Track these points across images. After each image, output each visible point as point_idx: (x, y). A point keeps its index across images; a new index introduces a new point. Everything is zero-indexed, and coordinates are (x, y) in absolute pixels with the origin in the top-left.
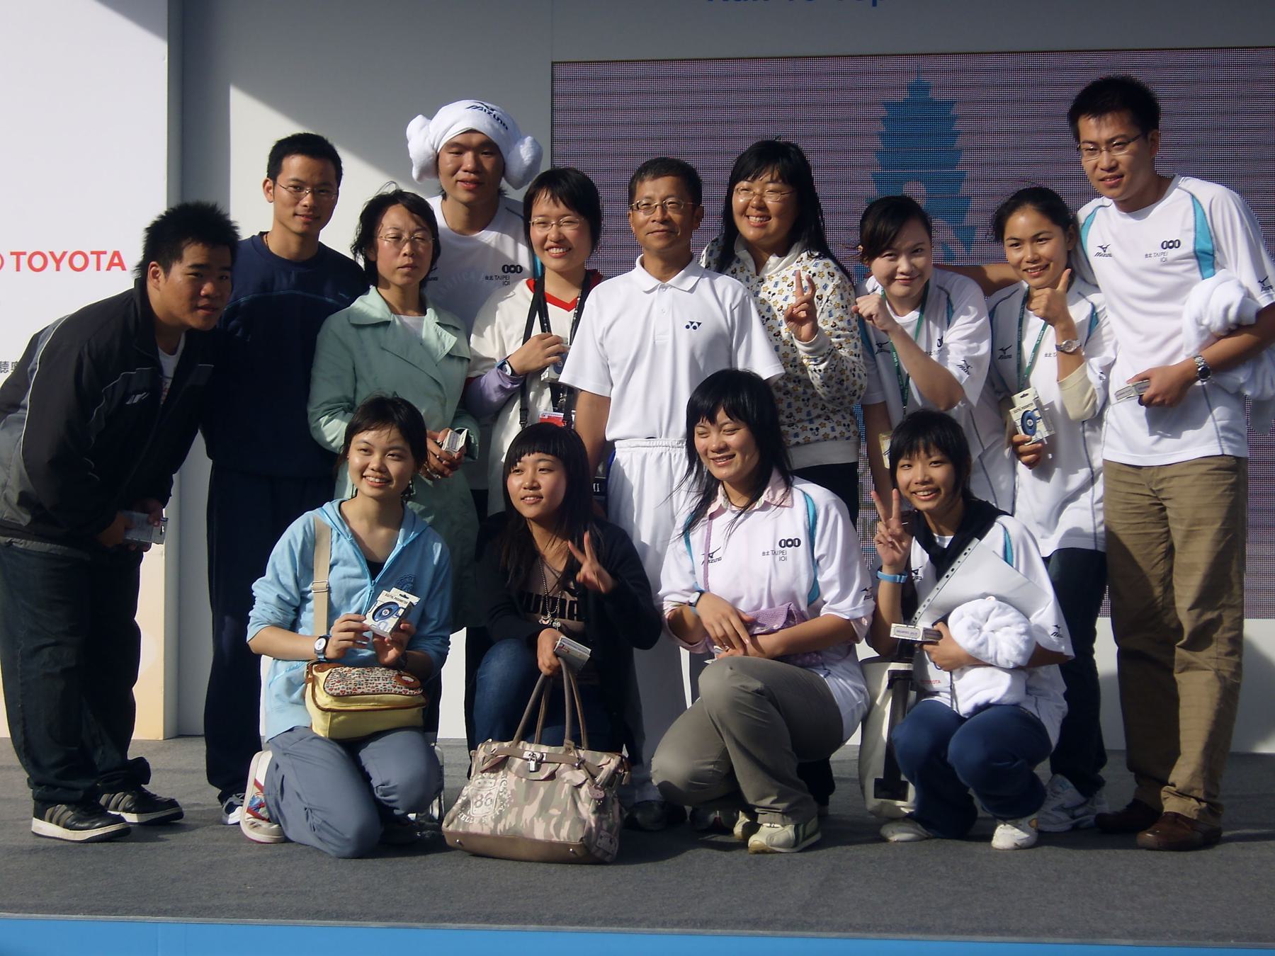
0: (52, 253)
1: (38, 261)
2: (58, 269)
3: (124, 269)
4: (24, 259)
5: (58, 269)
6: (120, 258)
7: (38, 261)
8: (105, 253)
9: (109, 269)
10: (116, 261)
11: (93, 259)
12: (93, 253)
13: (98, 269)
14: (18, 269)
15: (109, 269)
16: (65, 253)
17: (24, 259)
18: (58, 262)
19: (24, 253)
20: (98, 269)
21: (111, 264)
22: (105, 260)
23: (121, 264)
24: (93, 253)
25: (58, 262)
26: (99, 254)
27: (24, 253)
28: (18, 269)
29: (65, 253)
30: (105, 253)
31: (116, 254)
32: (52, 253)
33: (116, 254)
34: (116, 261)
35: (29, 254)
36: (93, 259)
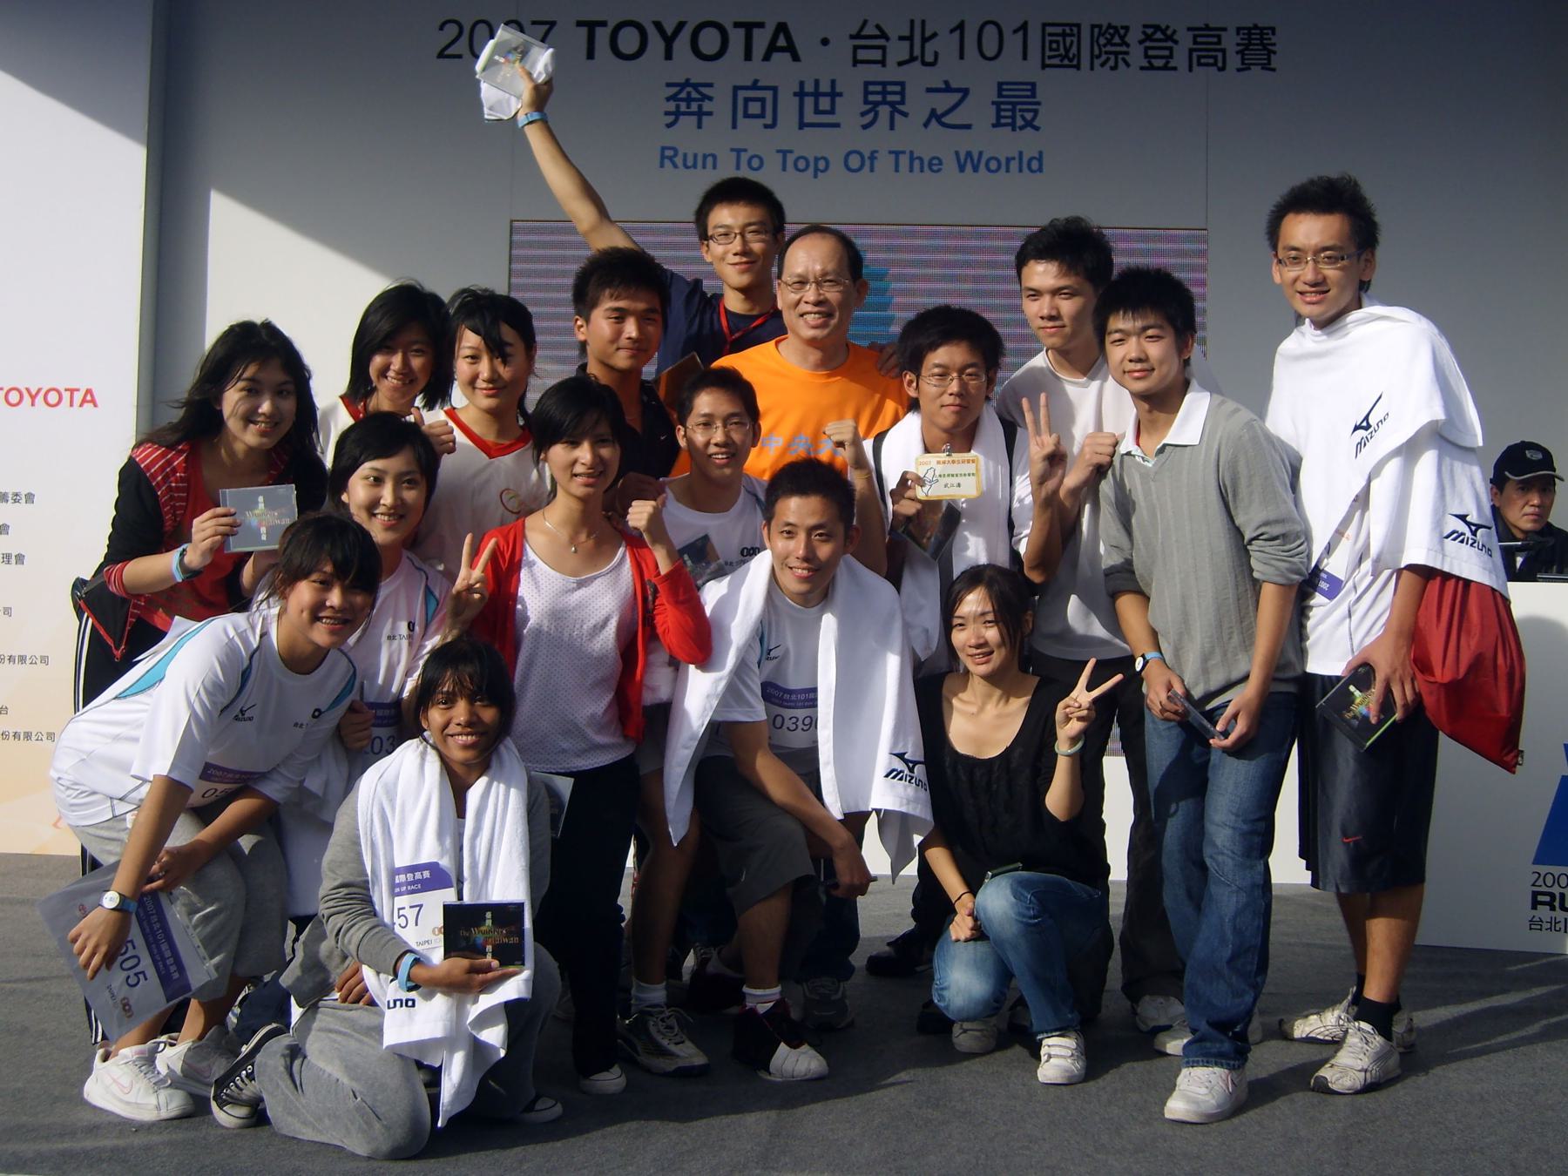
1: (628, 41)
2: (669, 56)
3: (796, 58)
4: (603, 35)
5: (669, 56)
6: (789, 38)
7: (628, 41)
8: (761, 25)
9: (767, 58)
10: (782, 42)
11: (736, 37)
12: (737, 25)
13: (748, 56)
14: (590, 55)
15: (767, 58)
16: (681, 25)
17: (603, 35)
18: (669, 41)
19: (603, 24)
20: (748, 56)
21: (772, 49)
22: (761, 39)
23: (791, 49)
24: (737, 25)
25: (669, 41)
26: (749, 27)
27: (603, 24)
28: (590, 55)
29: (681, 25)
30: (761, 25)
31: (782, 28)
33: (782, 28)
34: (782, 42)
35: (611, 25)
36: (736, 37)
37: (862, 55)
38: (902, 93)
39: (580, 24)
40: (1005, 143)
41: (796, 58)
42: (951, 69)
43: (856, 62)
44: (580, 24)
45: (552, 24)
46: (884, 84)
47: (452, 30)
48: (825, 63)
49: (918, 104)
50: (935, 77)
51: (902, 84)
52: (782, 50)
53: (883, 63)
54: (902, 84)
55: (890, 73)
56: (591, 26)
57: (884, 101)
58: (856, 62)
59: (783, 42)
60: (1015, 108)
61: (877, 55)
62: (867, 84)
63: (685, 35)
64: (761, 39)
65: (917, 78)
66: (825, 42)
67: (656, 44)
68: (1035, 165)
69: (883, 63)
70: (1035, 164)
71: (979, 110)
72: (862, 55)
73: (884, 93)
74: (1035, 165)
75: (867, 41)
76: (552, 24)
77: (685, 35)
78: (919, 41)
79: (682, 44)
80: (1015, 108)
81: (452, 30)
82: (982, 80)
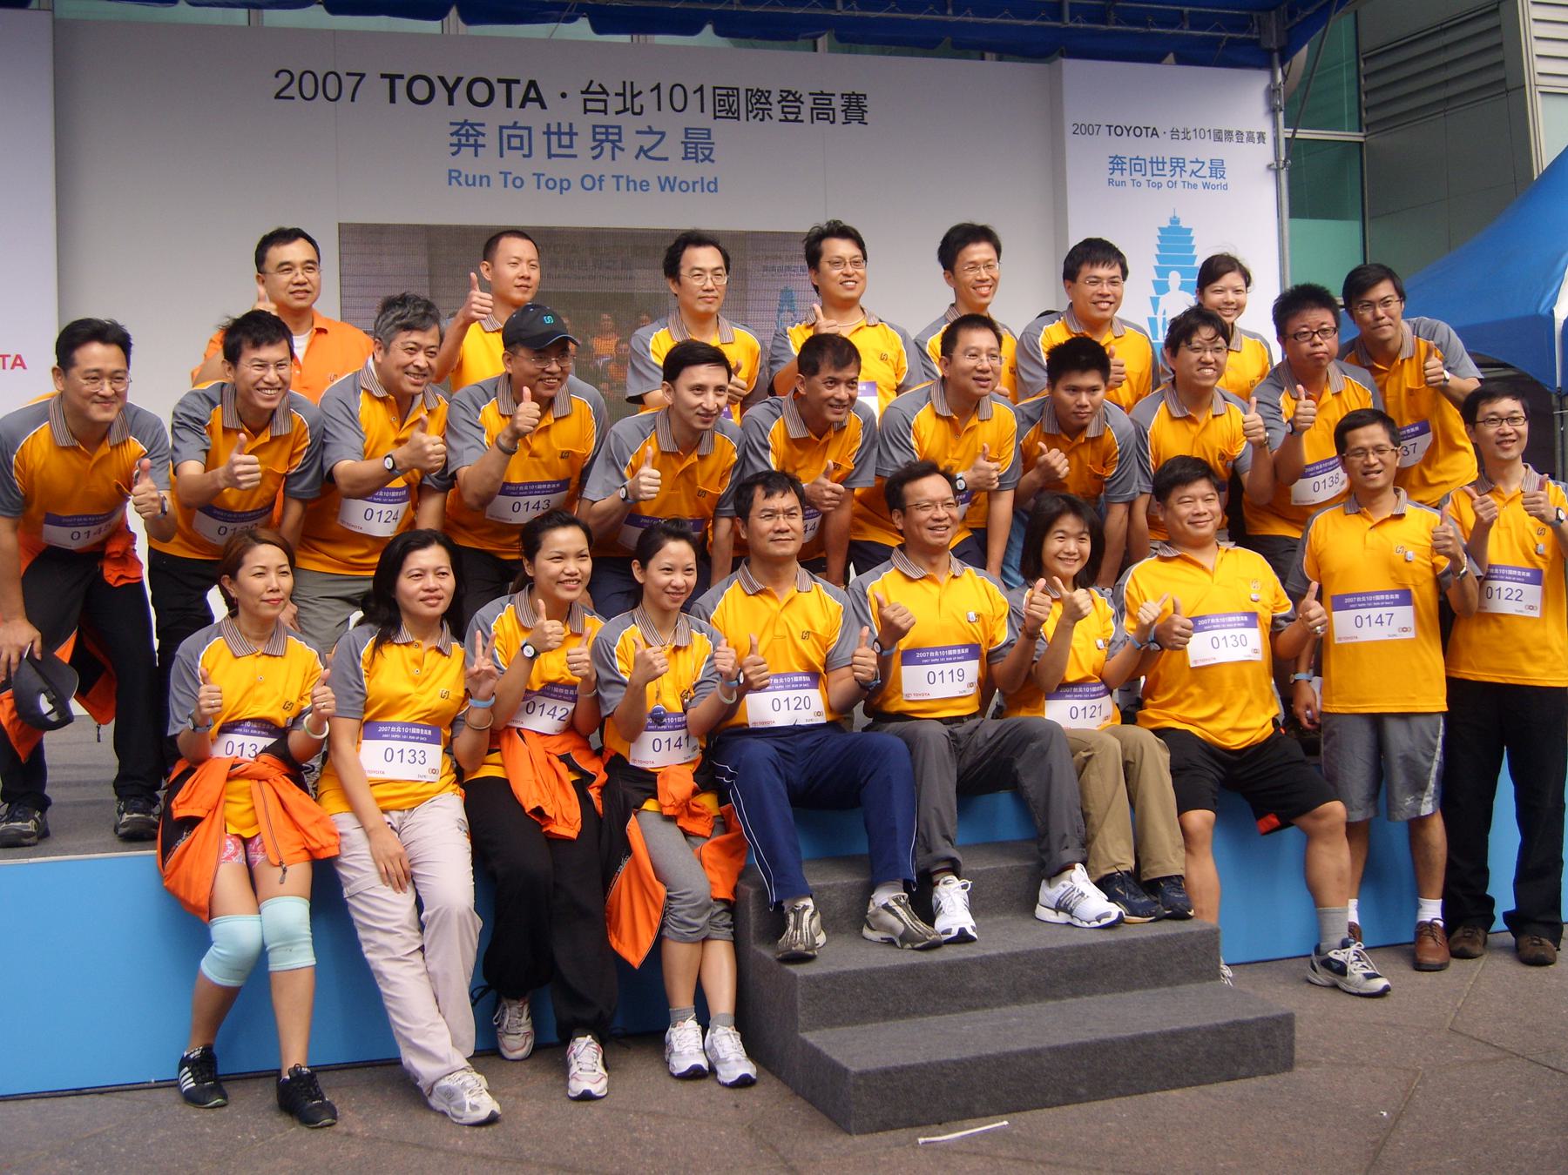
0: (442, 79)
1: (421, 90)
3: (543, 106)
4: (401, 86)
6: (537, 92)
7: (421, 90)
8: (517, 82)
9: (522, 106)
10: (533, 94)
11: (500, 90)
12: (500, 81)
13: (509, 105)
15: (522, 106)
16: (459, 80)
17: (401, 86)
18: (451, 91)
19: (401, 77)
20: (509, 105)
22: (518, 92)
24: (500, 81)
25: (451, 91)
26: (509, 83)
27: (401, 77)
29: (459, 80)
30: (517, 82)
32: (442, 79)
34: (533, 94)
36: (500, 90)
37: (590, 105)
38: (619, 134)
39: (383, 76)
40: (691, 171)
41: (543, 106)
42: (651, 118)
43: (586, 111)
44: (383, 76)
45: (362, 76)
46: (607, 127)
47: (285, 78)
48: (565, 112)
49: (631, 142)
50: (641, 123)
51: (619, 127)
52: (533, 100)
53: (605, 112)
54: (619, 127)
55: (611, 119)
56: (392, 78)
57: (607, 139)
58: (586, 111)
59: (533, 95)
60: (697, 146)
61: (601, 106)
62: (594, 127)
63: (463, 86)
64: (518, 92)
65: (627, 120)
66: (564, 95)
67: (441, 92)
68: (712, 187)
69: (605, 112)
70: (712, 186)
71: (673, 146)
72: (590, 105)
73: (607, 134)
74: (712, 187)
75: (593, 96)
76: (362, 76)
77: (463, 86)
78: (629, 94)
79: (461, 92)
80: (697, 146)
81: (285, 78)
82: (674, 125)
